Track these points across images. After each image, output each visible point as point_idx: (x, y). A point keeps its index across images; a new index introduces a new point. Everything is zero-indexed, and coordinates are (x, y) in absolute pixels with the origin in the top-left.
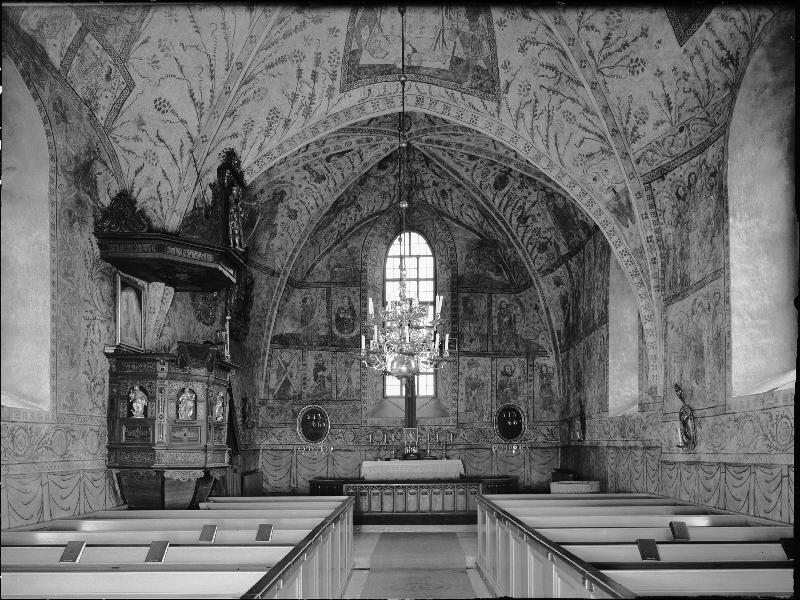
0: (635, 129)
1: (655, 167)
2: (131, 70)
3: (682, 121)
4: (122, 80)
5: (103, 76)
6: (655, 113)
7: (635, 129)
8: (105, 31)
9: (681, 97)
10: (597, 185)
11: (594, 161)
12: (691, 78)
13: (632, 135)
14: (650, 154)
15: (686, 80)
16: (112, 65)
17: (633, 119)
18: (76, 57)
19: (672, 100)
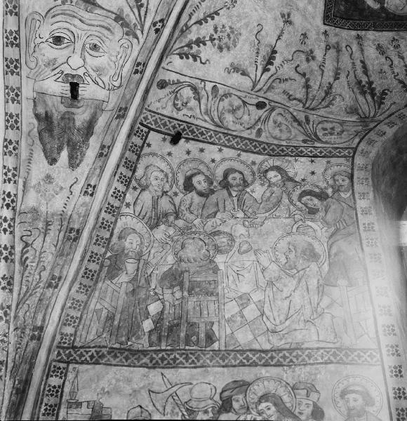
0: (199, 42)
1: (179, 116)
3: (270, 95)
6: (243, 52)
7: (199, 42)
9: (287, 71)
10: (49, 52)
11: (86, 16)
12: (314, 65)
13: (189, 45)
14: (187, 93)
15: (308, 60)
17: (206, 30)
19: (277, 61)
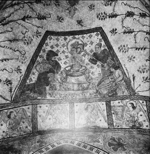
2: (141, 94)
4: (141, 101)
5: (131, 109)
8: (116, 94)
16: (132, 102)
18: (113, 115)
